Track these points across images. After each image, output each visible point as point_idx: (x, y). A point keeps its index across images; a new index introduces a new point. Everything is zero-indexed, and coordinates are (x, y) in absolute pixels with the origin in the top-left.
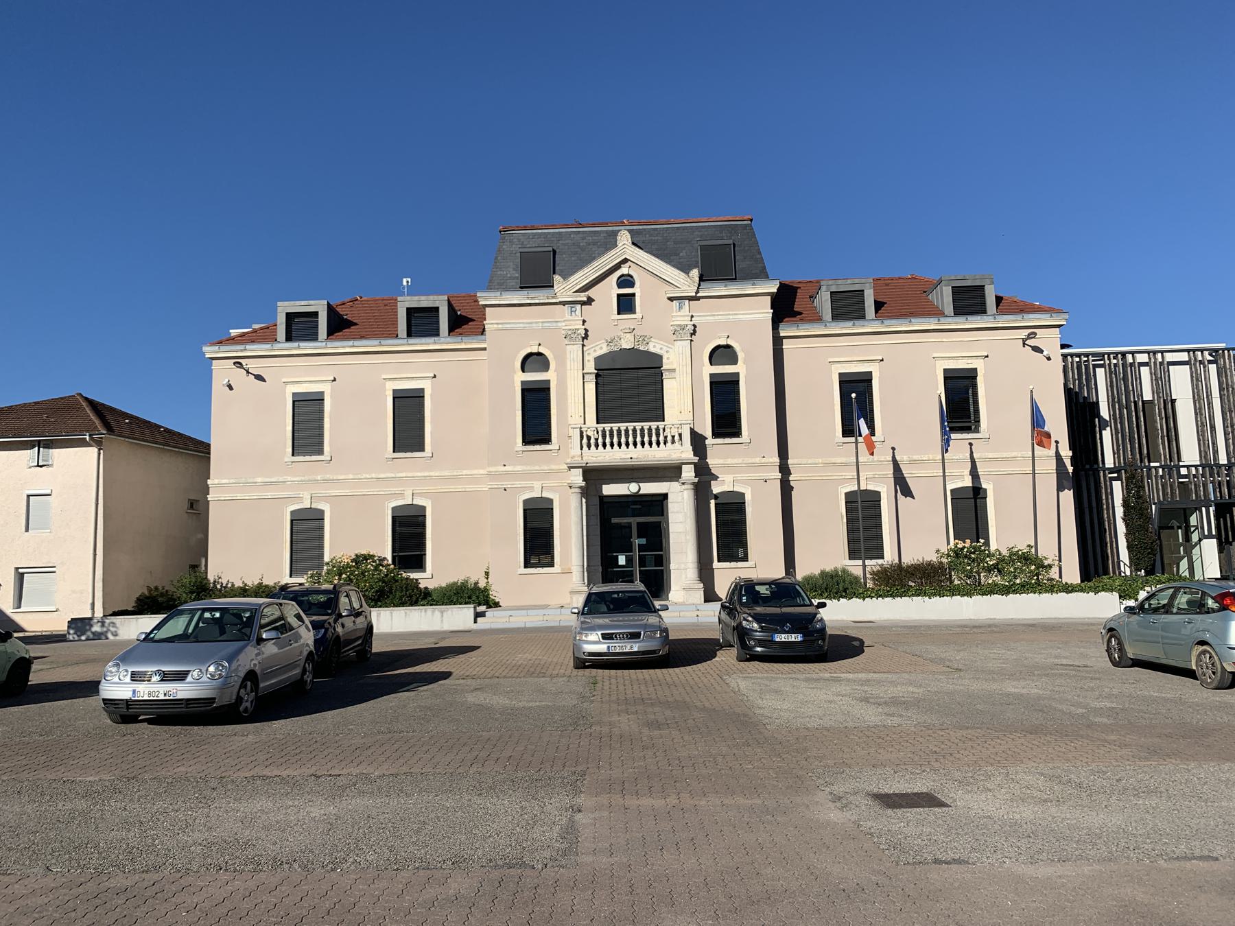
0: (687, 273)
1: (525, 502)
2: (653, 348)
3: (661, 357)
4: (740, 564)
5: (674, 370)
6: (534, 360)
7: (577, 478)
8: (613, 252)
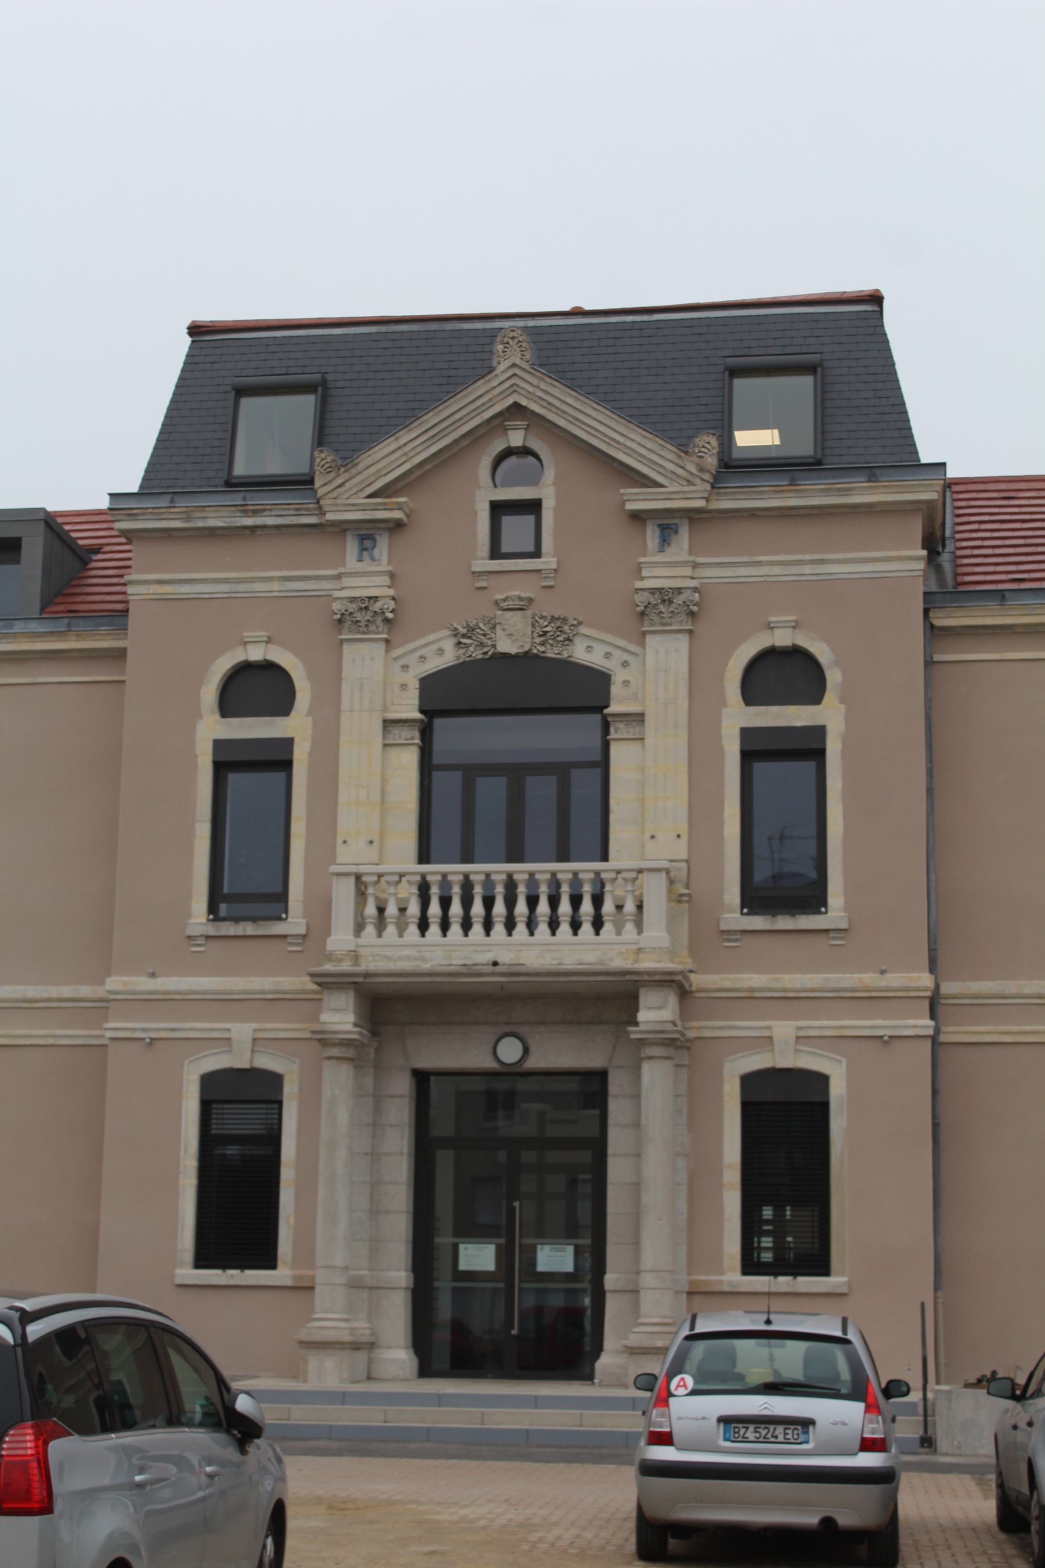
0: (684, 448)
2: (586, 652)
3: (601, 680)
5: (639, 718)
6: (255, 687)
7: (341, 1017)
8: (480, 387)
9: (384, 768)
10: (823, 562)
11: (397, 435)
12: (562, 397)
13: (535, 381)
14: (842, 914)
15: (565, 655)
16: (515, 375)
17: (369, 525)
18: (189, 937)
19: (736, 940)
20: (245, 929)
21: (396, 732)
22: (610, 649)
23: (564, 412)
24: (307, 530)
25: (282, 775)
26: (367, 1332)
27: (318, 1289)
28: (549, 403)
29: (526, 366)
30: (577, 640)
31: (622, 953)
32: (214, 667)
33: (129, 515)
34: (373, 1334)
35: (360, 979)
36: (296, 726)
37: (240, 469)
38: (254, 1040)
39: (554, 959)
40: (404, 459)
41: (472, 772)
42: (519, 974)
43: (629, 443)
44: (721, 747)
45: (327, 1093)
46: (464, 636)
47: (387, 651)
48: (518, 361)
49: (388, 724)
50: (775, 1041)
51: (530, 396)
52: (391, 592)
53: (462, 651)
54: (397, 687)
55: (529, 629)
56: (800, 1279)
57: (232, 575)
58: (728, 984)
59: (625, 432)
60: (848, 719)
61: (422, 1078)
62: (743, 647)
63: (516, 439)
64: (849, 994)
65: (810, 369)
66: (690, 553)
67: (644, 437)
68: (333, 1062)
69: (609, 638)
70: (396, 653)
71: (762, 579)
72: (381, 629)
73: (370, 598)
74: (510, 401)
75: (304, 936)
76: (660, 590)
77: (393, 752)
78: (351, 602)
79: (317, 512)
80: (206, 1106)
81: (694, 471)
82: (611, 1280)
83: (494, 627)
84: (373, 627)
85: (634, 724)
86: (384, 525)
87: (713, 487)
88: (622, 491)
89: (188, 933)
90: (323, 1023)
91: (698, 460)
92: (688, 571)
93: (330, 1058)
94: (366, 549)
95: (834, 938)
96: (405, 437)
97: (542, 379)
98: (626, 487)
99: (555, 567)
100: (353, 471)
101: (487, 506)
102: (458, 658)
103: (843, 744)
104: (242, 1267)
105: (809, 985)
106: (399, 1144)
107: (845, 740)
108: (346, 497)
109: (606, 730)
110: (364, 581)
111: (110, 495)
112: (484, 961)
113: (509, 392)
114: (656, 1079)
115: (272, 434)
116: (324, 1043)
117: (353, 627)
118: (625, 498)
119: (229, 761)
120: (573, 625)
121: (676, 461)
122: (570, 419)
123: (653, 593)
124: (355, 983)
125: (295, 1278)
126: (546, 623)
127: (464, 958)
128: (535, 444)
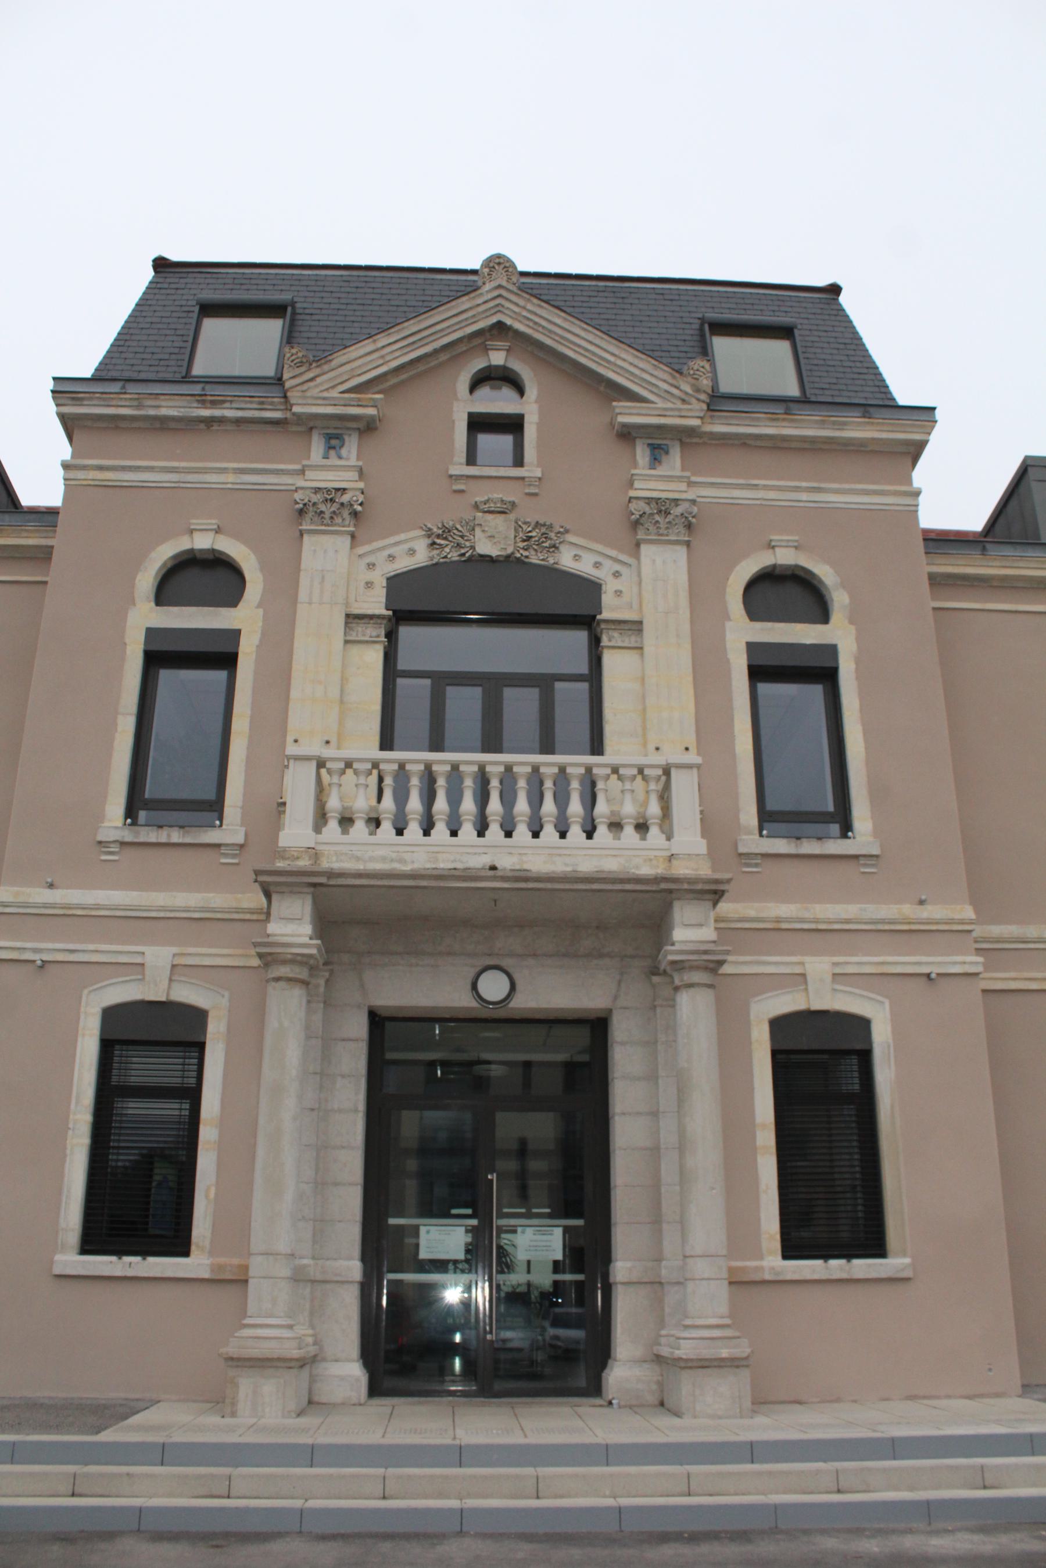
1: (110, 1014)
3: (592, 588)
4: (862, 1267)
5: (636, 627)
6: (199, 575)
7: (294, 927)
9: (344, 666)
10: (819, 490)
11: (375, 338)
12: (550, 318)
13: (521, 302)
14: (871, 839)
15: (551, 561)
16: (500, 296)
17: (338, 424)
18: (100, 842)
19: (756, 865)
20: (169, 836)
21: (360, 629)
22: (600, 559)
23: (550, 331)
24: (269, 428)
25: (222, 675)
26: (310, 1340)
27: (251, 1281)
28: (536, 323)
29: (515, 289)
30: (563, 548)
31: (651, 860)
32: (153, 555)
33: (73, 399)
34: (315, 1343)
35: (323, 880)
36: (245, 618)
37: (197, 370)
38: (173, 966)
39: (566, 865)
40: (381, 362)
41: (442, 681)
42: (526, 880)
43: (619, 362)
44: (728, 661)
45: (272, 1024)
46: (438, 536)
47: (352, 547)
48: (504, 283)
49: (352, 619)
50: (809, 978)
51: (517, 316)
52: (361, 485)
53: (436, 552)
54: (362, 584)
55: (512, 534)
56: (856, 1262)
57: (183, 464)
58: (752, 913)
59: (617, 352)
60: (858, 639)
61: (377, 1021)
62: (744, 564)
63: (497, 358)
64: (887, 927)
65: (785, 332)
66: (683, 469)
67: (637, 357)
68: (282, 984)
69: (600, 547)
70: (361, 550)
71: (758, 502)
72: (347, 522)
73: (337, 490)
74: (494, 320)
75: (242, 846)
76: (657, 500)
77: (355, 650)
78: (315, 493)
79: (282, 407)
80: (107, 1046)
81: (689, 390)
82: (621, 1269)
83: (473, 529)
84: (338, 520)
85: (630, 632)
86: (354, 425)
87: (709, 409)
88: (614, 404)
89: (99, 838)
90: (269, 936)
91: (693, 381)
92: (683, 486)
93: (278, 979)
94: (334, 448)
95: (865, 865)
96: (383, 340)
97: (529, 300)
98: (619, 401)
99: (540, 475)
100: (326, 367)
101: (466, 417)
102: (432, 558)
103: (857, 664)
104: (145, 1253)
105: (844, 916)
106: (351, 1097)
107: (858, 661)
108: (318, 394)
109: (595, 642)
110: (330, 475)
111: (54, 379)
112: (480, 866)
113: (493, 311)
114: (694, 1009)
115: (236, 347)
116: (268, 960)
117: (316, 519)
118: (617, 411)
119: (162, 656)
120: (559, 532)
121: (671, 381)
122: (557, 338)
123: (648, 504)
124: (314, 885)
125: (214, 1268)
126: (530, 529)
127: (454, 861)
128: (517, 366)
